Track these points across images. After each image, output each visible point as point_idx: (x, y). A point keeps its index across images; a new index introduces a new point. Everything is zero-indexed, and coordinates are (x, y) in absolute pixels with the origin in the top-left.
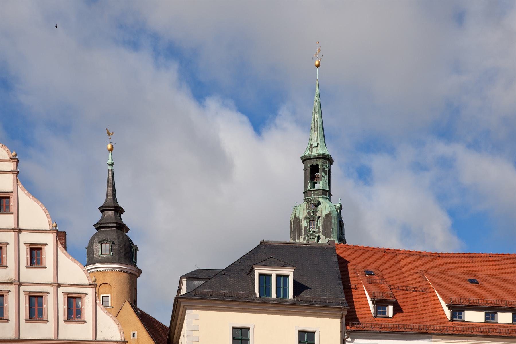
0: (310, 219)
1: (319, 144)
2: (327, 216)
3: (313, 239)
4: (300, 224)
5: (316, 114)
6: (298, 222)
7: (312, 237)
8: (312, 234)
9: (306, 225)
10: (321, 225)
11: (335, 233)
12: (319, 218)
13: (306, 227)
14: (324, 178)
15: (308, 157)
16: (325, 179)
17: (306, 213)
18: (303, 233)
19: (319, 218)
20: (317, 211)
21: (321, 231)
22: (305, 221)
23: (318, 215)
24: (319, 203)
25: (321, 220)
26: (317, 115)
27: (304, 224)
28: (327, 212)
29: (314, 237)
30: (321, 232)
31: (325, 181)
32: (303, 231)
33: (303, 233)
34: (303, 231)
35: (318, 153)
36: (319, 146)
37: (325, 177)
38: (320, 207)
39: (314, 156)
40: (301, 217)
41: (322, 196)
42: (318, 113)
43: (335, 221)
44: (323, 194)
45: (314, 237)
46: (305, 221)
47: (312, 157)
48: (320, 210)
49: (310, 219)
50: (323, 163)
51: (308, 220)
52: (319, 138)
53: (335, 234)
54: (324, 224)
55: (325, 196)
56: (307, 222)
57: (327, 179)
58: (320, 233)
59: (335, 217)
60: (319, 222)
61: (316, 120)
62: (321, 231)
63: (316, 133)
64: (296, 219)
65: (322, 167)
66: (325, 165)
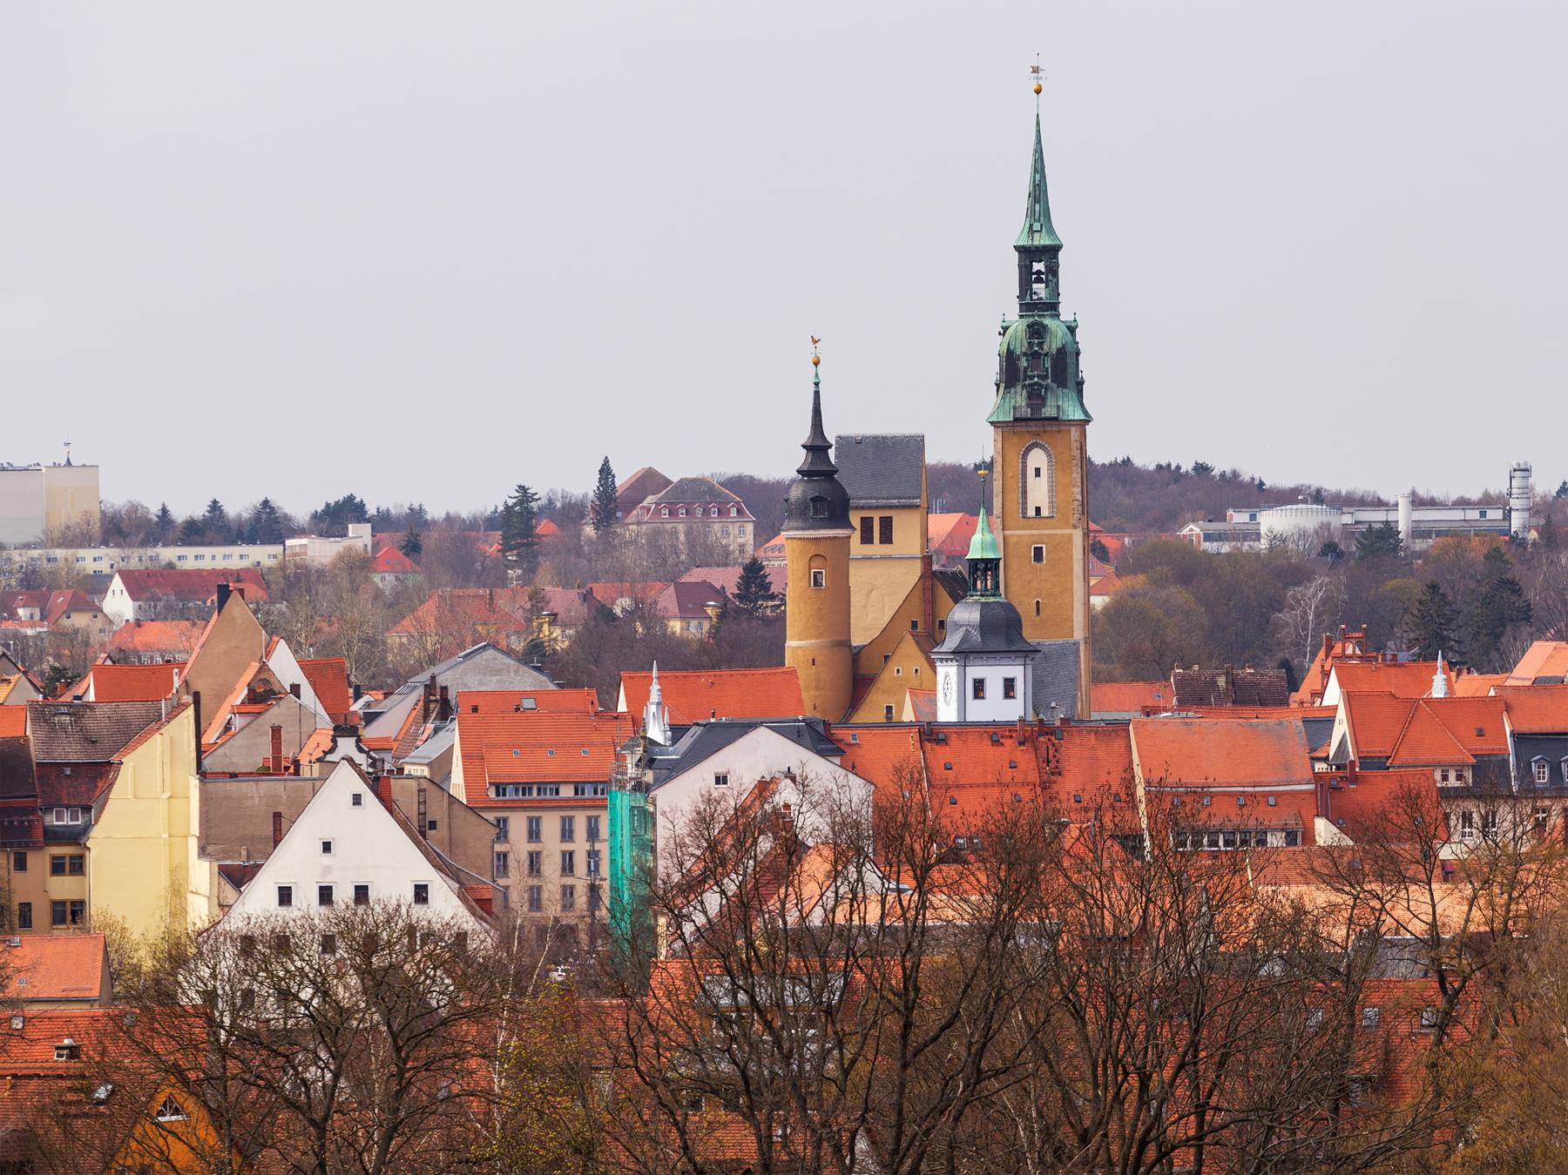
9: (1025, 365)
13: (1026, 369)
17: (1026, 345)
18: (1022, 377)
19: (1046, 355)
20: (1043, 343)
27: (1024, 363)
28: (1060, 345)
33: (1022, 377)
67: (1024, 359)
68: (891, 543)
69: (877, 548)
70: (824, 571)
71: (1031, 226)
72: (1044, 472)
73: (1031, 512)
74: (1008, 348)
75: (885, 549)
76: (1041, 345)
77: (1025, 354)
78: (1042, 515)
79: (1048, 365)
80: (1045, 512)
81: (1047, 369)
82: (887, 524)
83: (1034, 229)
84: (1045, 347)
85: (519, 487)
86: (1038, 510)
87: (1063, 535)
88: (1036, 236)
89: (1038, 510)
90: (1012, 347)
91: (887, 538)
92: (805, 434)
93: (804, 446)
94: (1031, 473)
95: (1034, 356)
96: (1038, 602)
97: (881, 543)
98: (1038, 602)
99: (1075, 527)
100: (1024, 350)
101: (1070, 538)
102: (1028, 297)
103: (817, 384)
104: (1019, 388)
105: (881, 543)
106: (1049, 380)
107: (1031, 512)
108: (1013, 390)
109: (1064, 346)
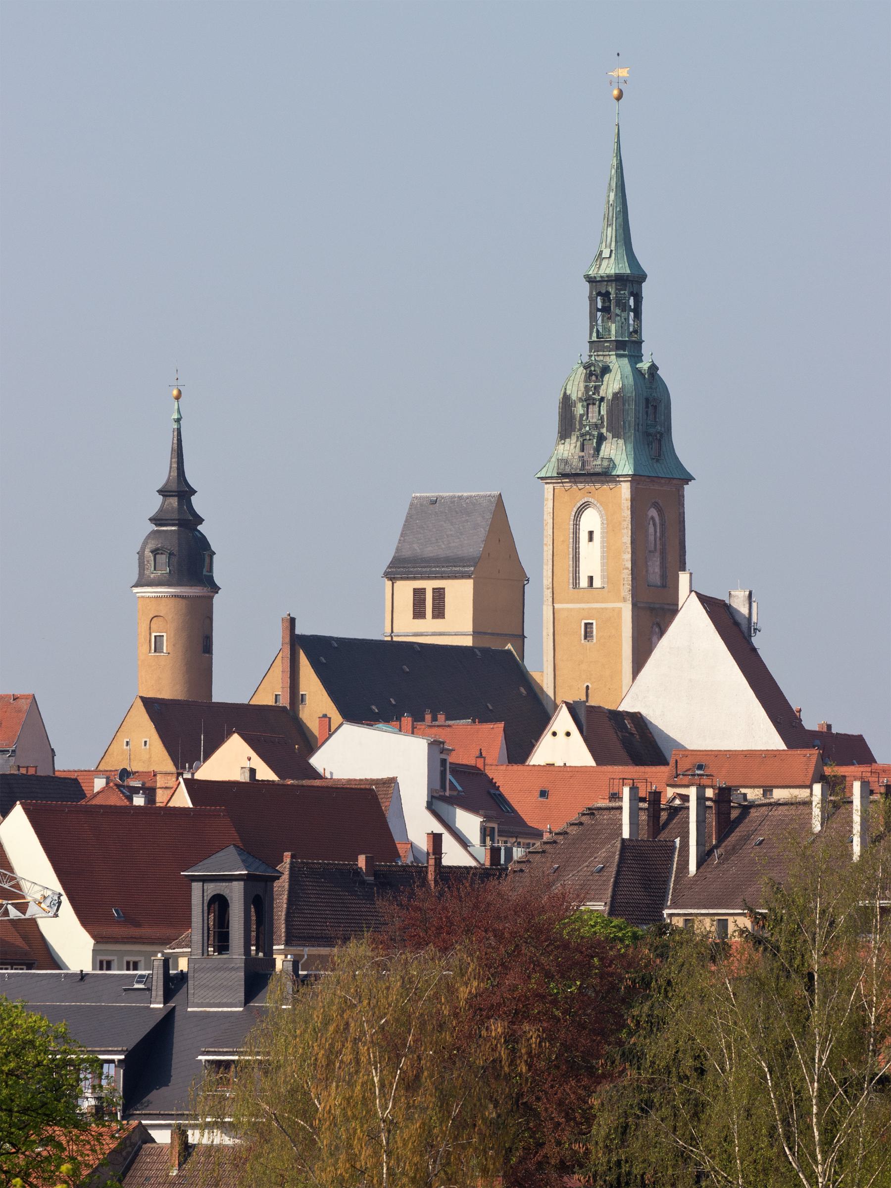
0: (588, 402)
2: (615, 395)
3: (591, 442)
7: (588, 437)
8: (587, 432)
9: (581, 412)
11: (629, 427)
12: (602, 399)
13: (581, 416)
14: (619, 318)
15: (591, 277)
19: (602, 399)
20: (599, 386)
21: (605, 424)
22: (581, 404)
24: (606, 370)
27: (579, 410)
29: (591, 438)
31: (622, 323)
32: (577, 423)
34: (577, 423)
35: (608, 272)
36: (613, 255)
37: (623, 315)
38: (607, 377)
39: (601, 277)
41: (614, 353)
43: (629, 405)
44: (617, 349)
45: (591, 438)
46: (581, 404)
47: (598, 279)
48: (605, 383)
49: (588, 402)
50: (617, 289)
51: (585, 404)
54: (610, 412)
58: (603, 428)
59: (629, 397)
60: (602, 408)
62: (605, 424)
64: (566, 398)
66: (622, 292)
67: (579, 405)
70: (164, 634)
72: (597, 536)
73: (584, 583)
74: (565, 393)
76: (597, 389)
77: (581, 400)
78: (595, 585)
80: (597, 583)
81: (603, 415)
82: (439, 594)
83: (603, 256)
86: (591, 579)
87: (613, 609)
89: (591, 579)
90: (568, 392)
91: (439, 612)
92: (162, 474)
93: (160, 492)
94: (584, 536)
95: (589, 401)
96: (587, 687)
97: (434, 617)
98: (587, 687)
99: (625, 600)
100: (580, 395)
101: (620, 611)
103: (178, 421)
105: (434, 617)
106: (605, 429)
107: (584, 583)
108: (568, 440)
109: (622, 389)
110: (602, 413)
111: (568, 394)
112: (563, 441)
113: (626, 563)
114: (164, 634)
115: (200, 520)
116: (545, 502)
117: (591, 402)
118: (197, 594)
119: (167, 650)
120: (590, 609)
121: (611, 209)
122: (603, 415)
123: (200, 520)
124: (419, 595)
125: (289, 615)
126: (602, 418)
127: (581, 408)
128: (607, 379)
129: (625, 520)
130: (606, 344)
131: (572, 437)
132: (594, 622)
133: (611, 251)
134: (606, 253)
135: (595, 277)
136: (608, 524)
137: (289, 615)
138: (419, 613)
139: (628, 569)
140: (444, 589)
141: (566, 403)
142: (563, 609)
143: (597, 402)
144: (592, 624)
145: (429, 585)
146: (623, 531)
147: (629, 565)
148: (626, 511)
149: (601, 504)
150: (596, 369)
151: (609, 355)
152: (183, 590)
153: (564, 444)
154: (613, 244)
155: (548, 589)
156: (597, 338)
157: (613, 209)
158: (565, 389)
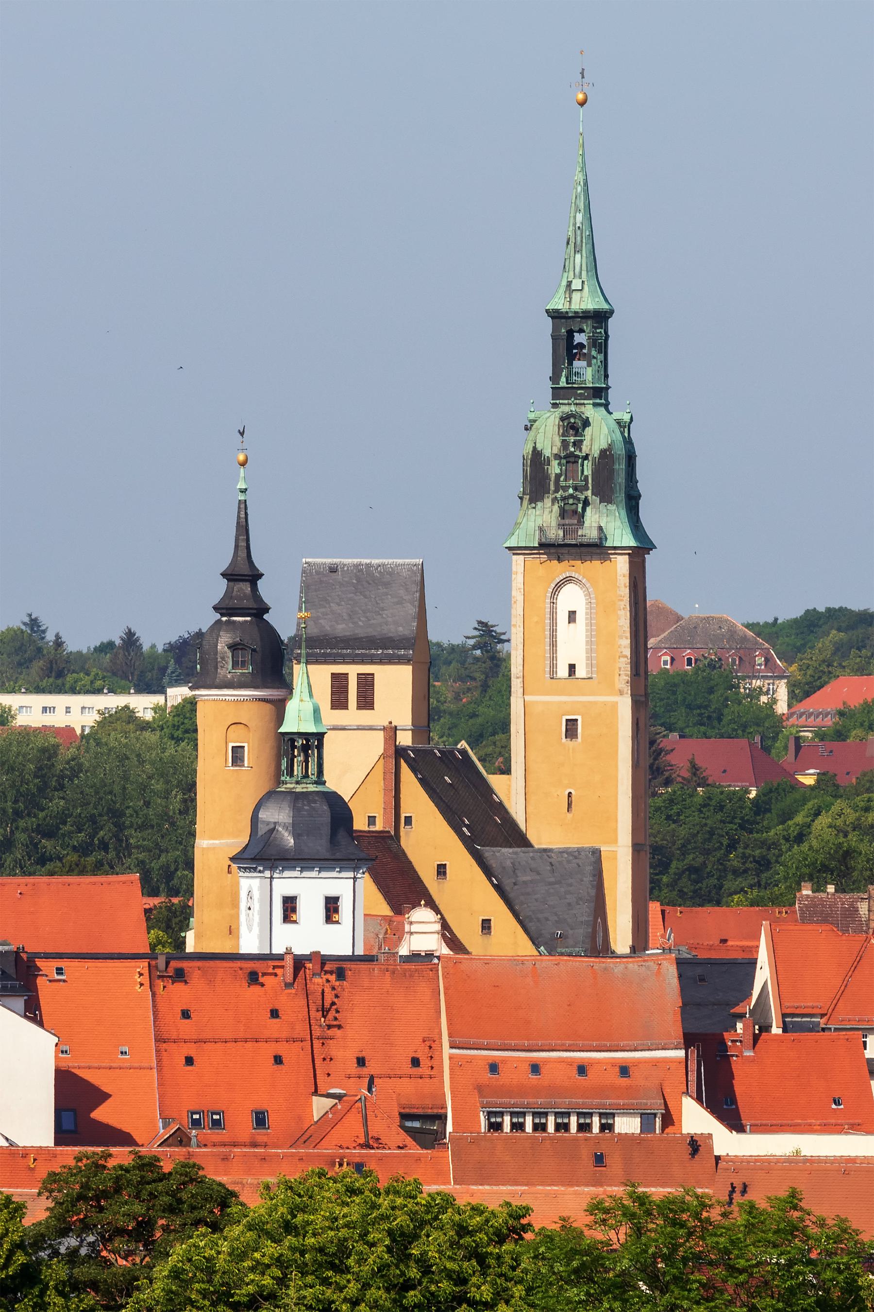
1: (586, 283)
2: (603, 452)
4: (546, 467)
5: (578, 214)
6: (541, 463)
9: (558, 471)
10: (590, 473)
11: (620, 490)
13: (558, 476)
14: (595, 360)
15: (562, 312)
16: (599, 361)
17: (559, 444)
18: (552, 488)
19: (586, 457)
20: (582, 441)
21: (590, 485)
22: (557, 462)
23: (585, 449)
24: (586, 423)
25: (590, 463)
26: (581, 214)
27: (555, 468)
28: (604, 446)
29: (576, 502)
30: (591, 488)
31: (599, 367)
32: (552, 484)
33: (552, 488)
34: (552, 484)
36: (586, 287)
37: (599, 357)
39: (575, 313)
40: (547, 453)
41: (591, 402)
42: (582, 211)
43: (619, 465)
46: (557, 462)
47: (570, 315)
49: (568, 459)
50: (593, 327)
51: (563, 461)
52: (584, 267)
53: (620, 494)
55: (598, 401)
56: (559, 464)
57: (601, 362)
58: (587, 489)
59: (619, 455)
61: (579, 227)
62: (590, 485)
63: (578, 256)
64: (536, 454)
65: (593, 336)
66: (598, 331)
67: (555, 463)
68: (373, 709)
69: (352, 715)
71: (569, 284)
72: (580, 617)
74: (535, 448)
75: (365, 717)
76: (578, 444)
77: (557, 457)
79: (588, 471)
80: (580, 672)
81: (587, 477)
82: (366, 684)
83: (573, 287)
84: (584, 448)
85: (480, 622)
86: (572, 668)
87: (605, 704)
88: (576, 296)
89: (572, 668)
90: (539, 447)
91: (366, 701)
94: (562, 617)
95: (570, 459)
97: (359, 707)
98: (570, 793)
99: (621, 693)
100: (555, 451)
102: (563, 379)
104: (548, 502)
105: (359, 707)
106: (589, 493)
108: (539, 504)
109: (610, 447)
110: (586, 473)
111: (539, 449)
112: (533, 505)
113: (623, 650)
114: (245, 745)
115: (267, 610)
116: (514, 576)
117: (572, 459)
118: (280, 698)
119: (249, 763)
120: (574, 702)
121: (579, 232)
122: (587, 477)
123: (267, 610)
124: (339, 683)
125: (390, 723)
126: (586, 479)
127: (556, 466)
128: (590, 433)
129: (622, 600)
130: (579, 392)
131: (546, 500)
132: (579, 718)
133: (583, 282)
134: (576, 284)
135: (567, 312)
136: (597, 604)
137: (390, 723)
138: (339, 701)
139: (626, 657)
140: (373, 674)
141: (537, 460)
142: (537, 702)
143: (580, 461)
144: (576, 720)
145: (353, 671)
146: (619, 612)
147: (627, 652)
148: (623, 589)
149: (588, 580)
150: (577, 421)
151: (584, 404)
152: (279, 693)
153: (534, 508)
154: (584, 273)
155: (518, 678)
156: (567, 383)
157: (582, 233)
158: (535, 443)
